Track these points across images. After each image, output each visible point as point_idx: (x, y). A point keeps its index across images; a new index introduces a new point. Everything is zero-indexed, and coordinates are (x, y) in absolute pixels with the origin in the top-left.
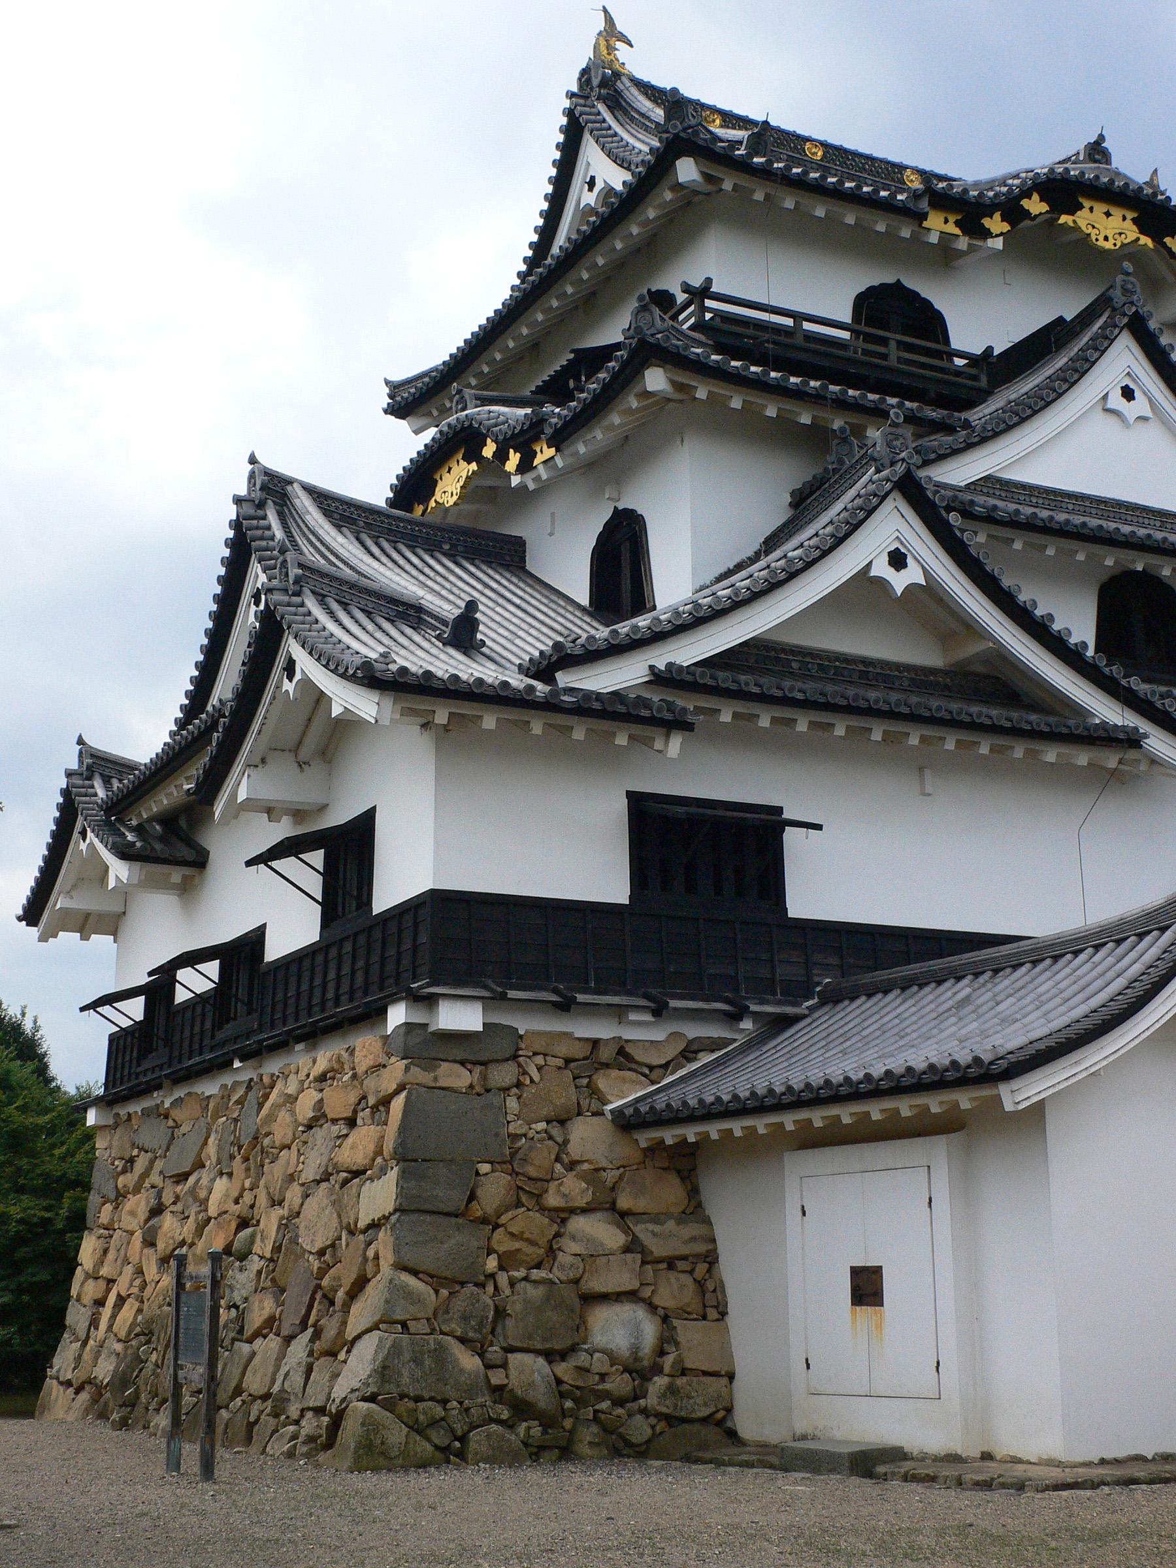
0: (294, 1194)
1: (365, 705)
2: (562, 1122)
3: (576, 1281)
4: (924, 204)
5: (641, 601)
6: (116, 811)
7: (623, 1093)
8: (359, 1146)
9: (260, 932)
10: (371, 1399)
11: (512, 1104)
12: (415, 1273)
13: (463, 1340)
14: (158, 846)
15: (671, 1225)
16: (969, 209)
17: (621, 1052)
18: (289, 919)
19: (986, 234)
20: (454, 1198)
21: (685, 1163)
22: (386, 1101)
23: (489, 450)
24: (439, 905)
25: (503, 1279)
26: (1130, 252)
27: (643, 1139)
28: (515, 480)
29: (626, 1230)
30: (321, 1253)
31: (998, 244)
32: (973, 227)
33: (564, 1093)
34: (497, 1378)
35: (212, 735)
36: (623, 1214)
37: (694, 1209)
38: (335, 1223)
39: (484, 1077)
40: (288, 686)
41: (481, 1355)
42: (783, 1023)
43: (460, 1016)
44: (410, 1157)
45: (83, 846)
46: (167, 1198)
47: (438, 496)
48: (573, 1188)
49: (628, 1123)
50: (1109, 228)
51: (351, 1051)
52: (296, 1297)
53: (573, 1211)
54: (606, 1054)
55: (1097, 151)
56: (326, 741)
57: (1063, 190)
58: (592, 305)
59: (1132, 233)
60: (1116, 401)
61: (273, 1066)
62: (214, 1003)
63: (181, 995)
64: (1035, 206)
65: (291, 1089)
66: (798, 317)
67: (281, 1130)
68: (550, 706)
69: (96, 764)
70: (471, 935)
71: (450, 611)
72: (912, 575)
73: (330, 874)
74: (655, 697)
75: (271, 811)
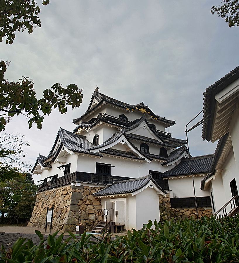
0: (59, 202)
1: (71, 153)
2: (88, 195)
3: (88, 212)
4: (126, 107)
5: (98, 144)
6: (43, 161)
7: (94, 193)
8: (67, 197)
9: (57, 175)
10: (67, 224)
11: (83, 193)
12: (72, 211)
13: (76, 218)
14: (47, 165)
15: (98, 206)
16: (130, 107)
17: (94, 188)
18: (61, 174)
19: (132, 111)
20: (76, 203)
21: (100, 200)
22: (70, 193)
23: (84, 128)
24: (78, 173)
25: (81, 212)
26: (145, 113)
27: (96, 197)
28: (86, 131)
29: (93, 207)
30: (62, 209)
31: (133, 111)
32: (131, 110)
33: (88, 193)
34: (80, 222)
35: (53, 155)
36: (93, 205)
37: (100, 205)
38: (64, 205)
39: (80, 191)
40: (63, 150)
41: (78, 220)
42: (110, 186)
43: (78, 184)
44: (72, 199)
45: (39, 165)
46: (45, 202)
48: (89, 202)
49: (94, 196)
50: (143, 111)
51: (67, 187)
52: (59, 213)
53: (88, 205)
54: (92, 189)
55: (142, 103)
56: (67, 156)
57: (139, 107)
58: (94, 114)
59: (145, 111)
60: (143, 127)
61: (58, 189)
62: (52, 182)
63: (48, 181)
64: (136, 108)
65: (60, 191)
66: (114, 117)
67: (58, 196)
68: (89, 154)
69: (41, 157)
70: (81, 176)
71: (80, 144)
72: (124, 143)
73: (65, 169)
74: (99, 153)
75: (60, 163)
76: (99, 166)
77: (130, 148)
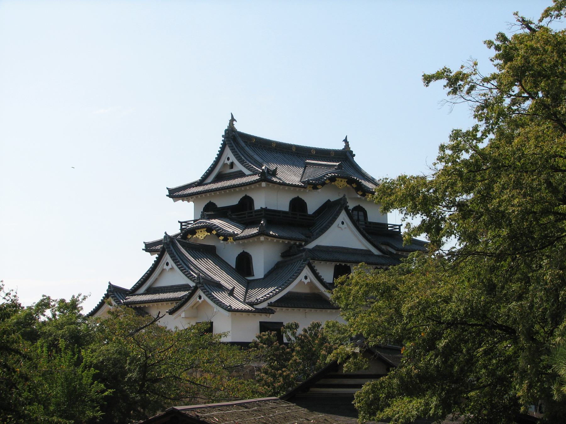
47: (197, 235)
59: (346, 184)
60: (341, 225)
72: (308, 280)
76: (264, 326)
77: (316, 288)
